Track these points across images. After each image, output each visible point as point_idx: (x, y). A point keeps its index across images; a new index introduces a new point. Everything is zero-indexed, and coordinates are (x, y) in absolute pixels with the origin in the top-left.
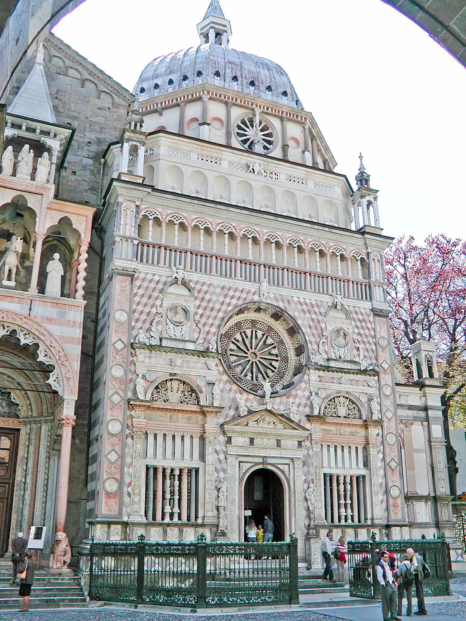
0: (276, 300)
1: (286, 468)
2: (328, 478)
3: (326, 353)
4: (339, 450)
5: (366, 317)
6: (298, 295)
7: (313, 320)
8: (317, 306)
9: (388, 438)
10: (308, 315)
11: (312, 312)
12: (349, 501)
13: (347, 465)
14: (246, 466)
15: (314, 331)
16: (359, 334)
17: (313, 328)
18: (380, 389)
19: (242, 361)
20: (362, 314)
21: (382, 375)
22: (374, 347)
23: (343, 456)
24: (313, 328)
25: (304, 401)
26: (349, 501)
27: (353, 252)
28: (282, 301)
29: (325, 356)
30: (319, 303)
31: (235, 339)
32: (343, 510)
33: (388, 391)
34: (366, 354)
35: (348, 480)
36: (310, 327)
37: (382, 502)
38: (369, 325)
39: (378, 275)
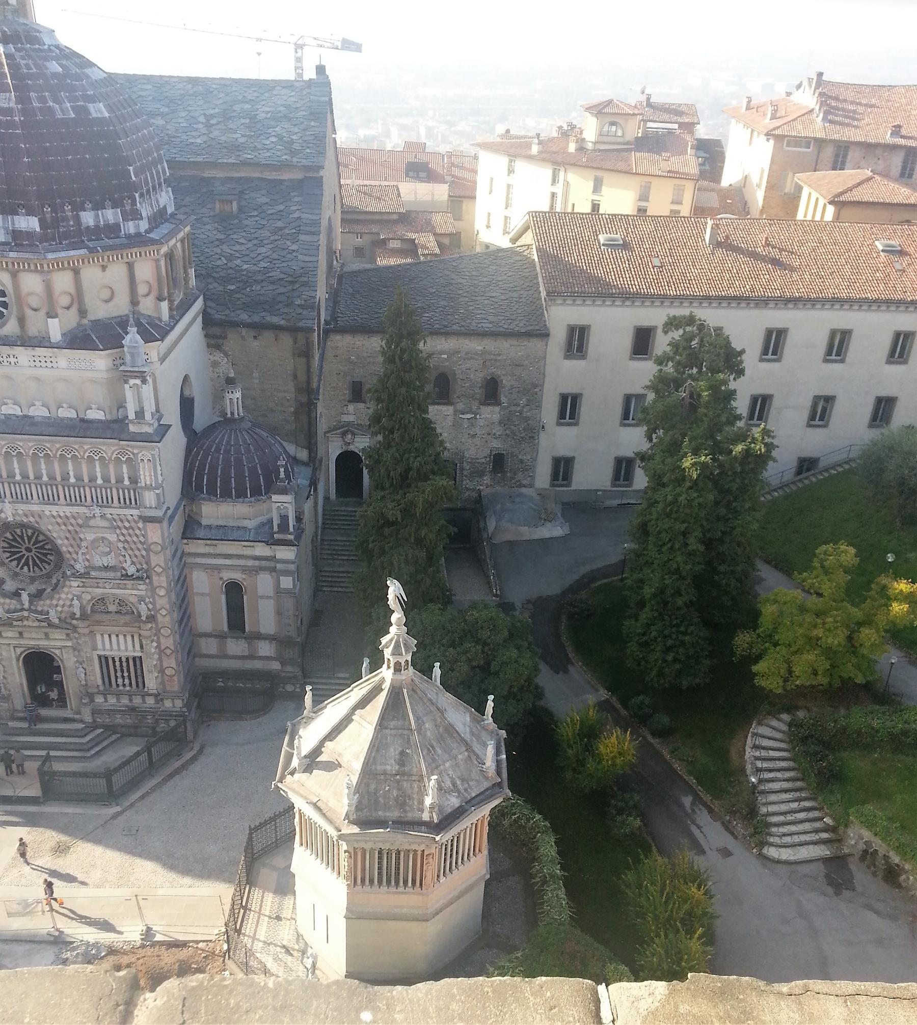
0: (26, 516)
1: (57, 652)
2: (103, 660)
3: (88, 560)
4: (114, 638)
5: (133, 524)
6: (48, 510)
7: (69, 531)
8: (75, 518)
9: (162, 631)
10: (63, 527)
11: (68, 524)
12: (126, 674)
13: (123, 647)
14: (19, 651)
15: (73, 542)
16: (128, 542)
17: (71, 539)
18: (153, 590)
19: (17, 556)
20: (128, 521)
21: (155, 578)
22: (144, 553)
23: (118, 641)
24: (71, 539)
25: (68, 603)
26: (126, 674)
27: (116, 453)
28: (33, 516)
29: (87, 564)
30: (76, 515)
31: (5, 538)
32: (120, 681)
33: (162, 592)
34: (134, 559)
35: (124, 659)
36: (67, 538)
37: (156, 678)
38: (138, 532)
39: (148, 478)
